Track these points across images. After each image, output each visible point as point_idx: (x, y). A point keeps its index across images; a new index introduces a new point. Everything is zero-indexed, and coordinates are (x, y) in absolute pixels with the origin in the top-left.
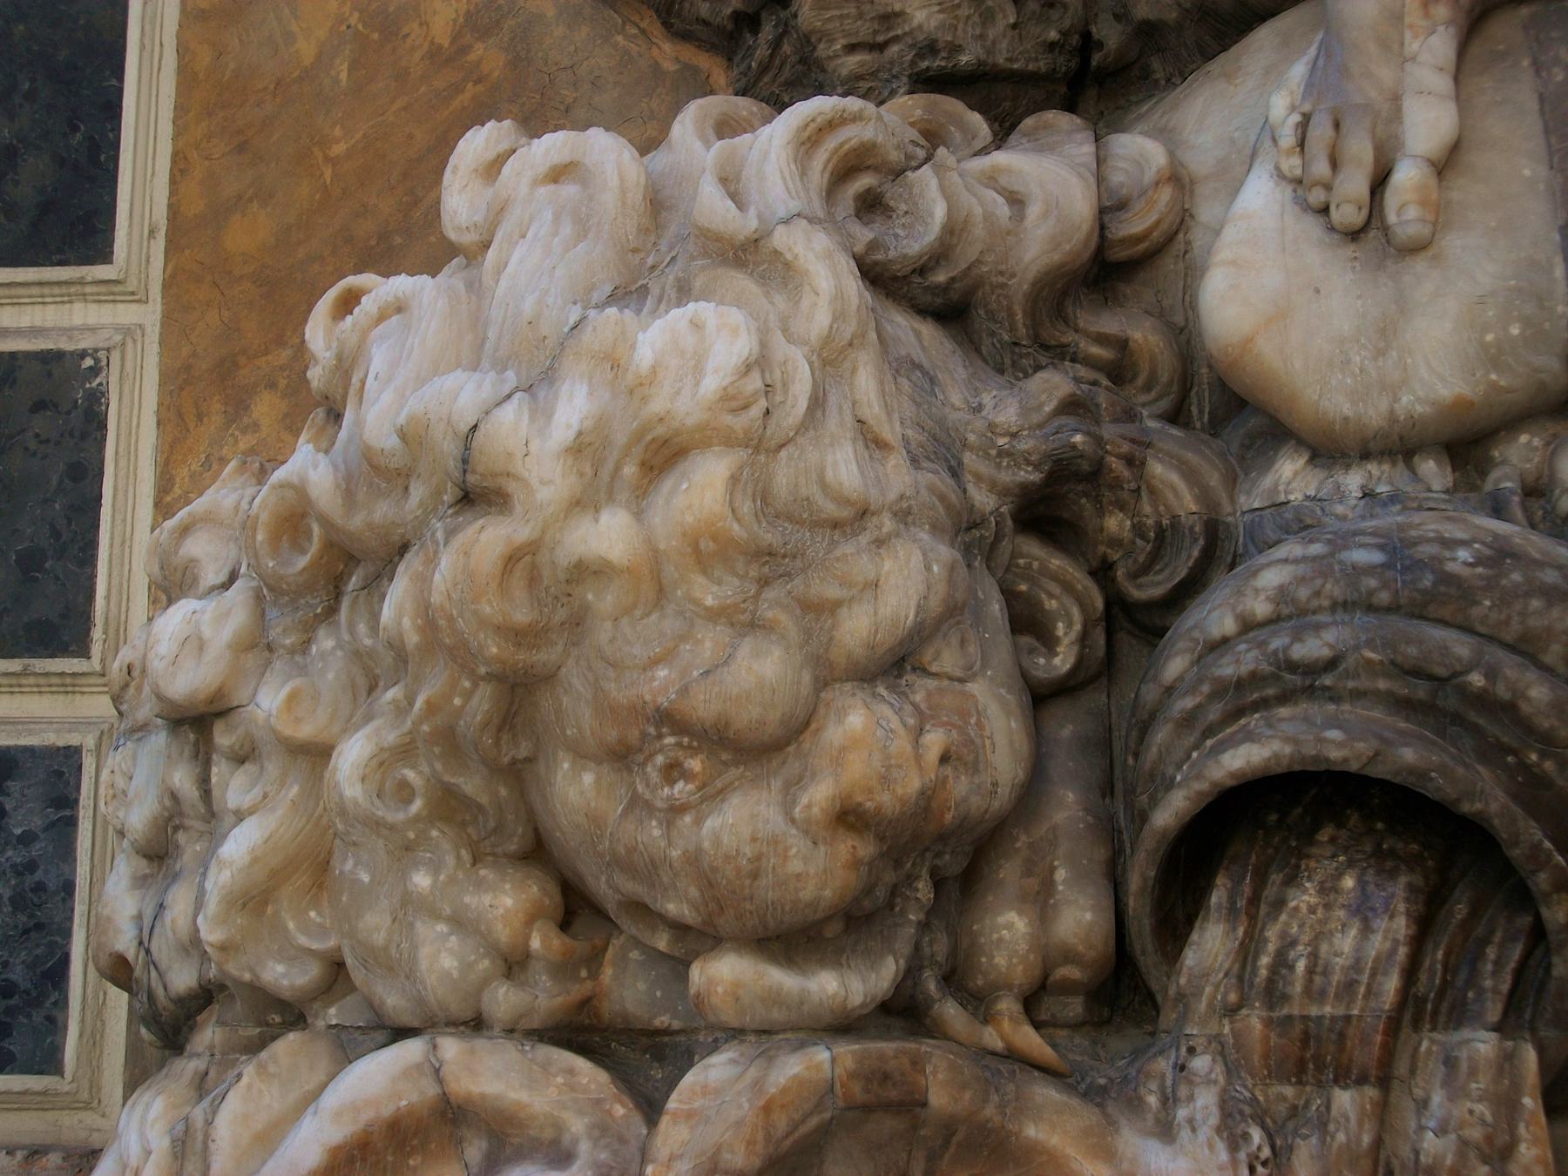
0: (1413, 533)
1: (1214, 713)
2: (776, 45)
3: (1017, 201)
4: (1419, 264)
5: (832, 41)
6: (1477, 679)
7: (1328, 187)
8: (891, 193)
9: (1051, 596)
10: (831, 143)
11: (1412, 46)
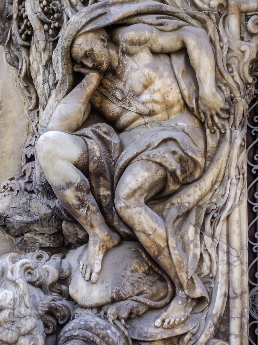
0: (88, 320)
1: (65, 340)
2: (22, 240)
3: (48, 272)
4: (94, 286)
5: (29, 242)
6: (92, 339)
7: (85, 275)
8: (32, 272)
9: (49, 323)
10: (25, 266)
11: (96, 257)
